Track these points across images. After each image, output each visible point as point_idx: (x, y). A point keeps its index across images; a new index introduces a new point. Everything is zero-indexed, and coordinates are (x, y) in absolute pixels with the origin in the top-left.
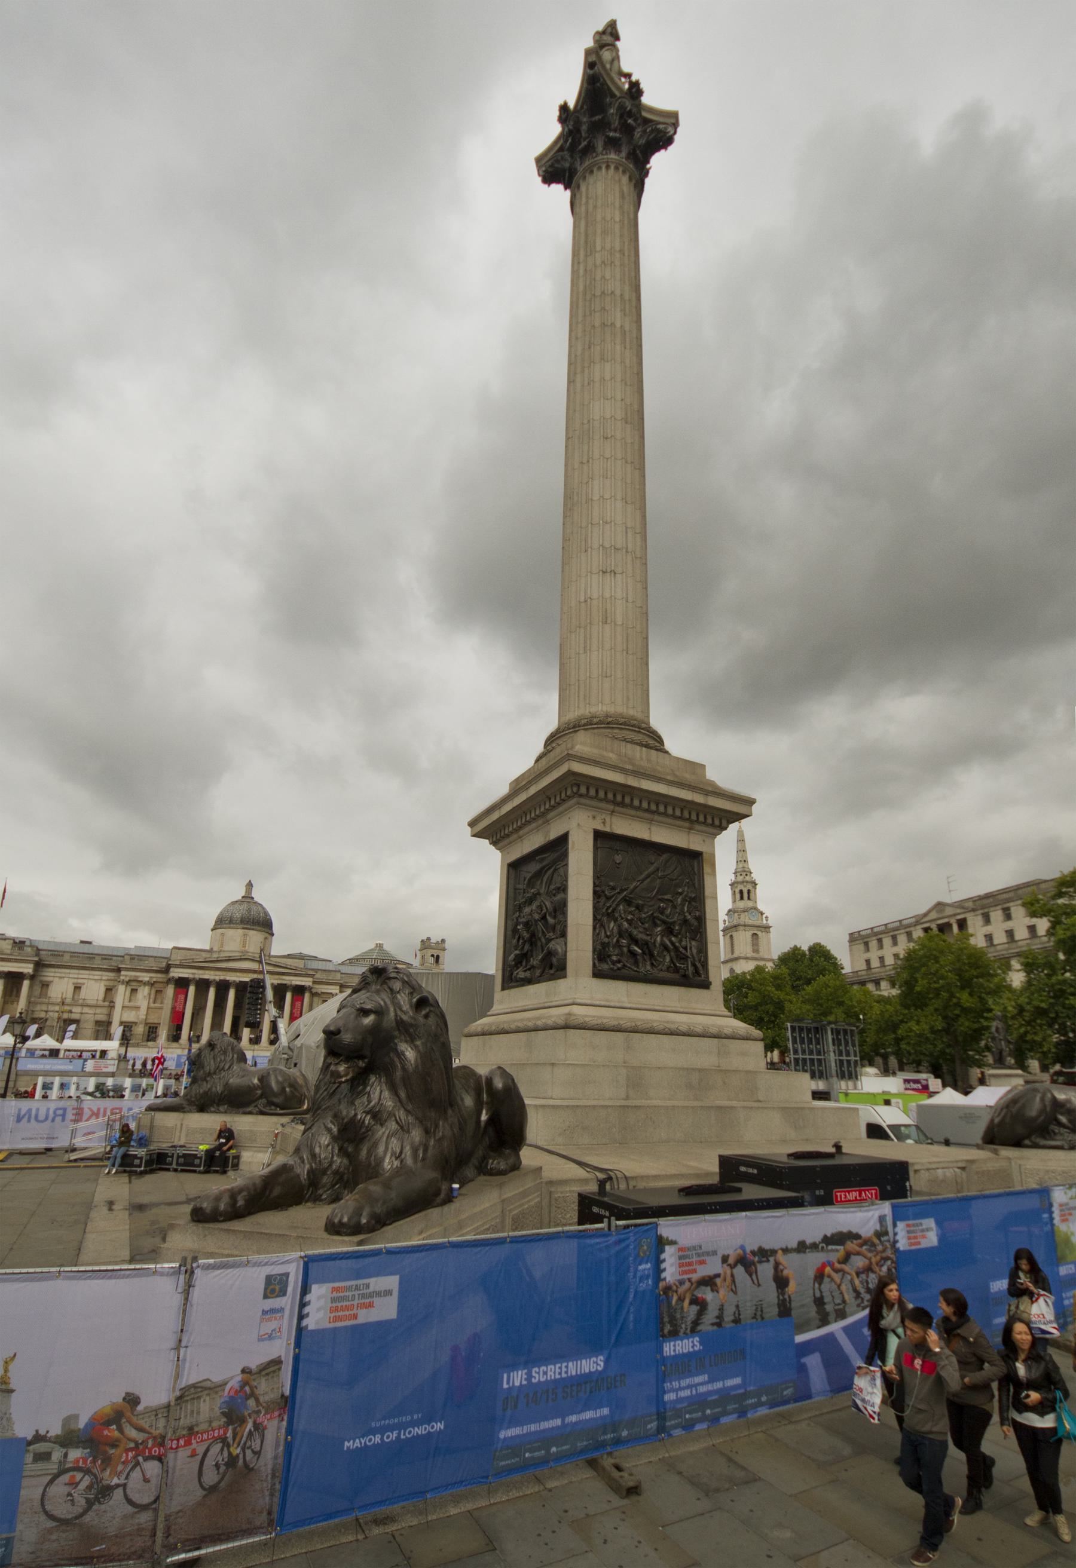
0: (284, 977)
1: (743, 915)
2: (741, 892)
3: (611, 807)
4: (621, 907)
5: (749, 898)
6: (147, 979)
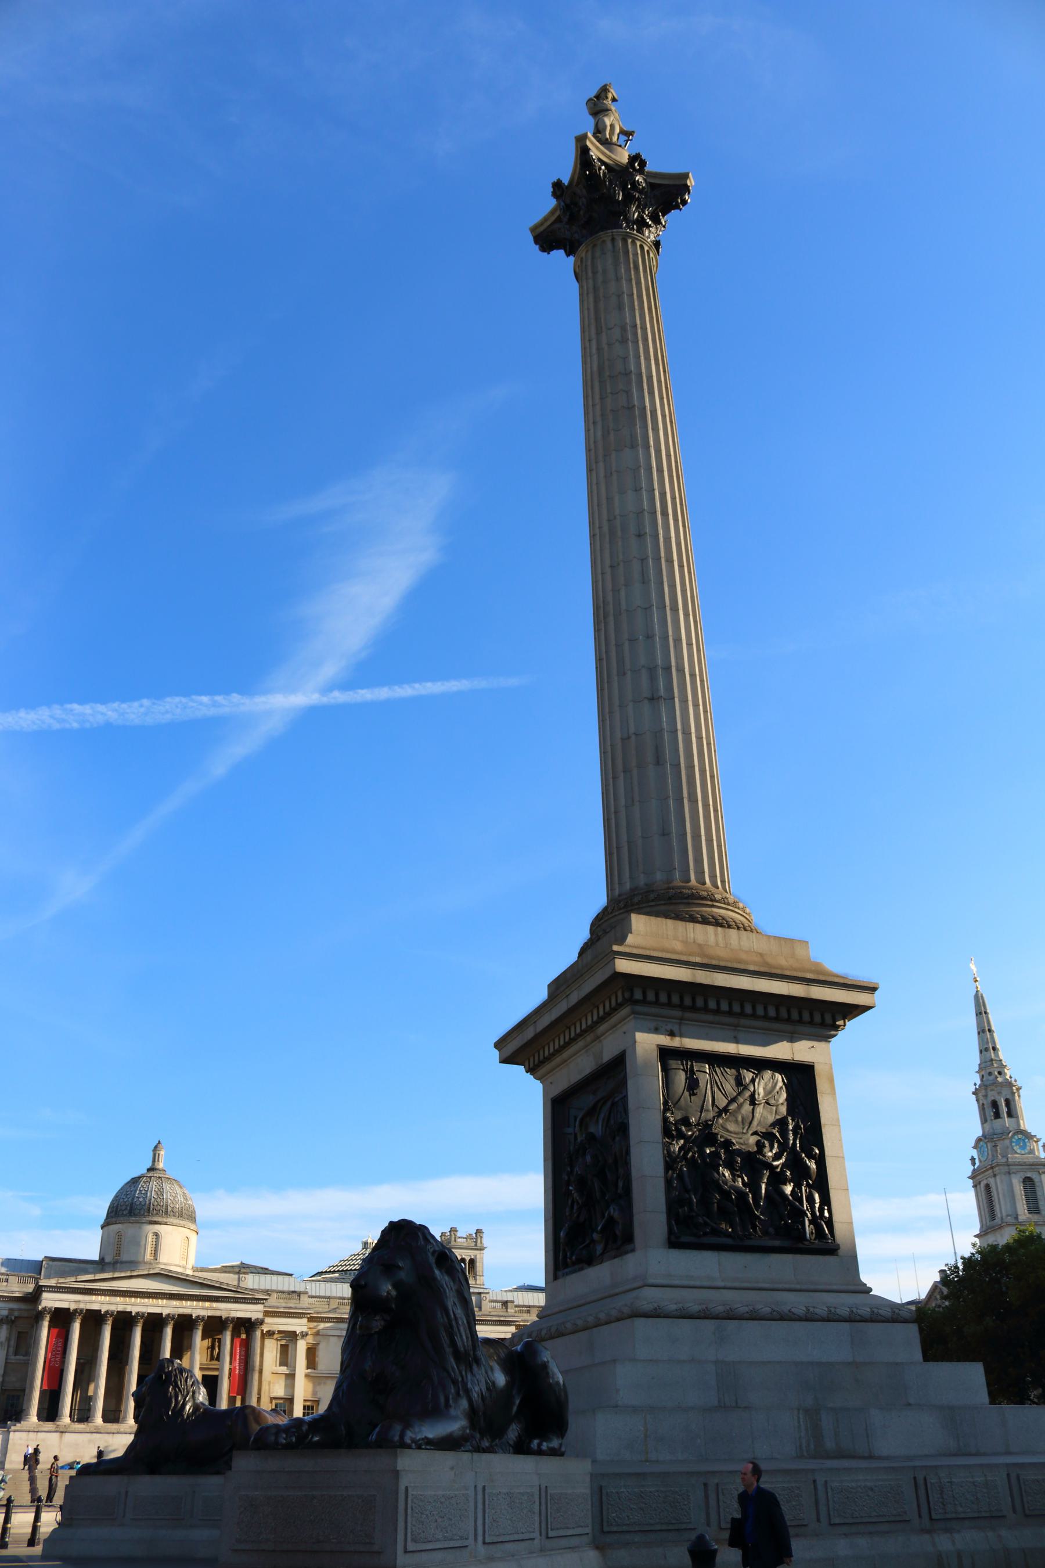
3: (678, 1013)
6: (5, 1313)
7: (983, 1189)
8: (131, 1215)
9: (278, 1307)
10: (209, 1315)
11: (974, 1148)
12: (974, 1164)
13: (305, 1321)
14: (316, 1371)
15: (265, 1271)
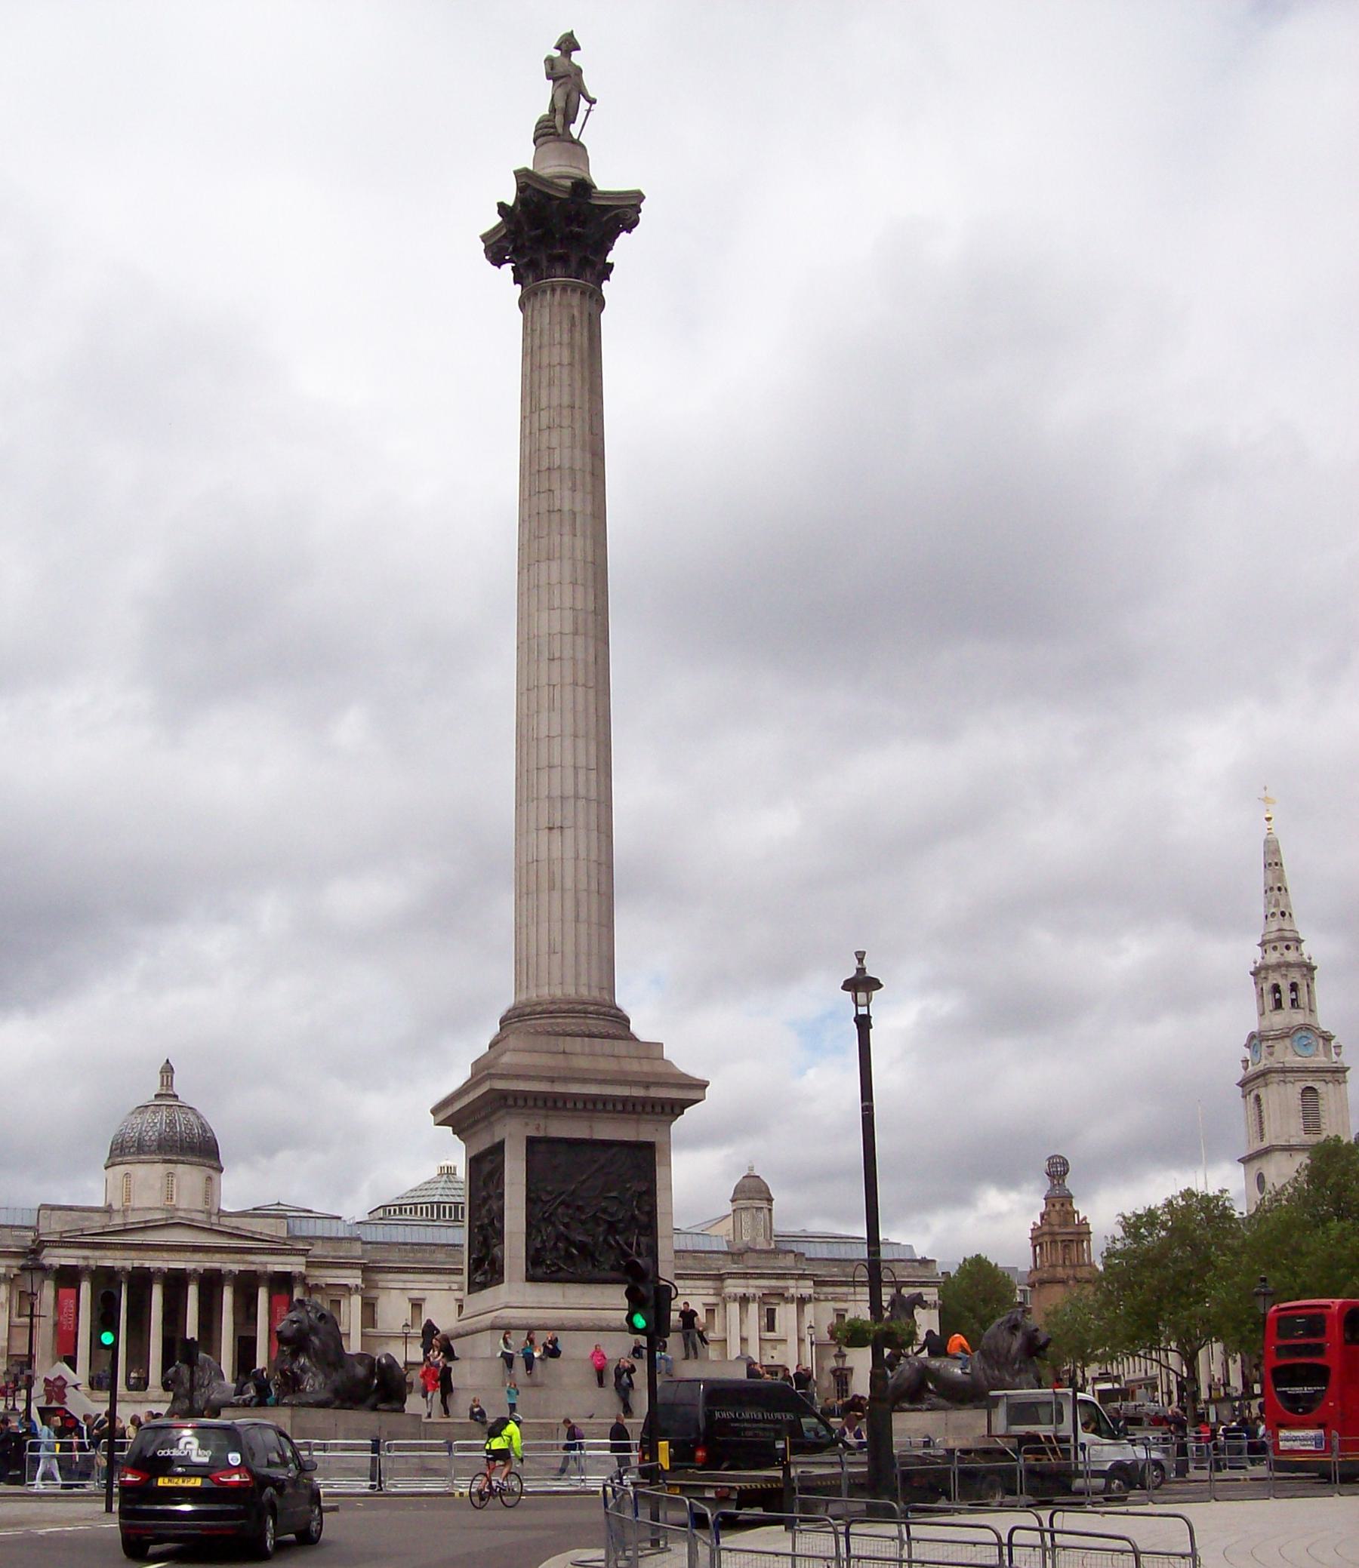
1: (1279, 1047)
2: (1276, 989)
3: (543, 1112)
4: (560, 1210)
5: (1294, 1003)
7: (1252, 1100)
8: (139, 1154)
9: (326, 1257)
11: (1248, 1046)
12: (1246, 1068)
14: (375, 1330)
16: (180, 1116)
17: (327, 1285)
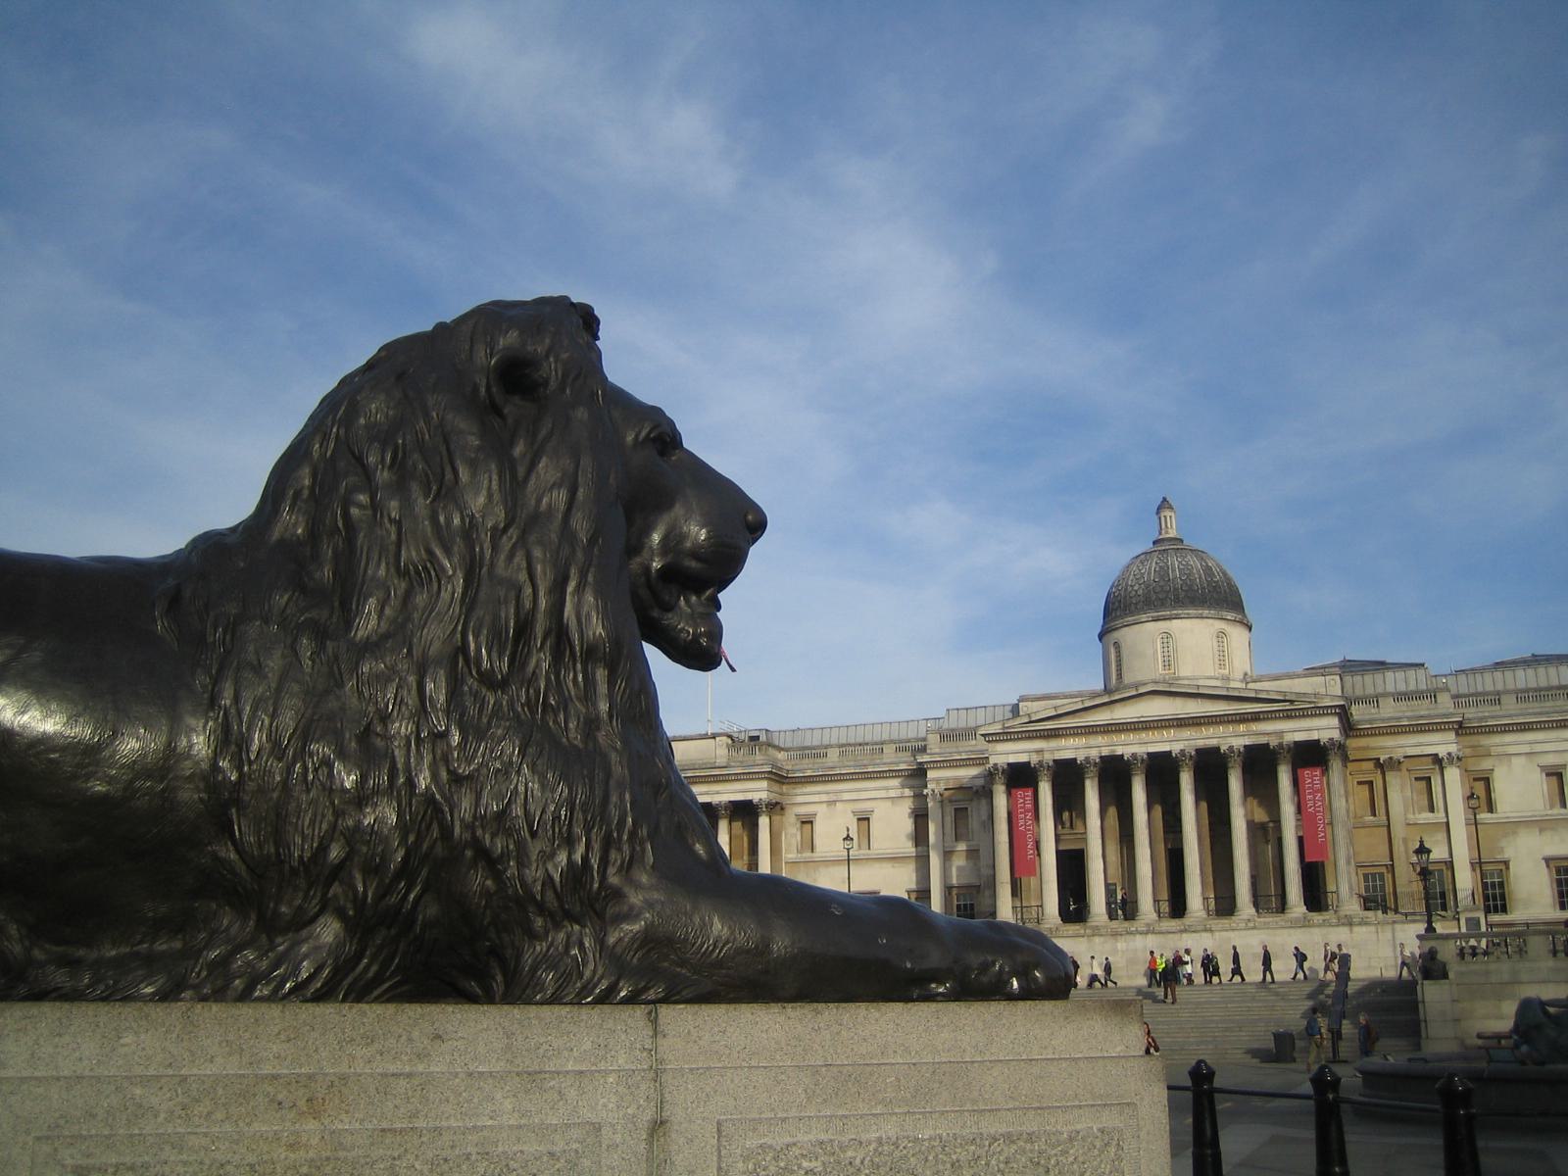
0: (1255, 727)
9: (1399, 719)
10: (1247, 743)
13: (1452, 736)
14: (1494, 815)
15: (1381, 666)
16: (1174, 561)
17: (1405, 757)
